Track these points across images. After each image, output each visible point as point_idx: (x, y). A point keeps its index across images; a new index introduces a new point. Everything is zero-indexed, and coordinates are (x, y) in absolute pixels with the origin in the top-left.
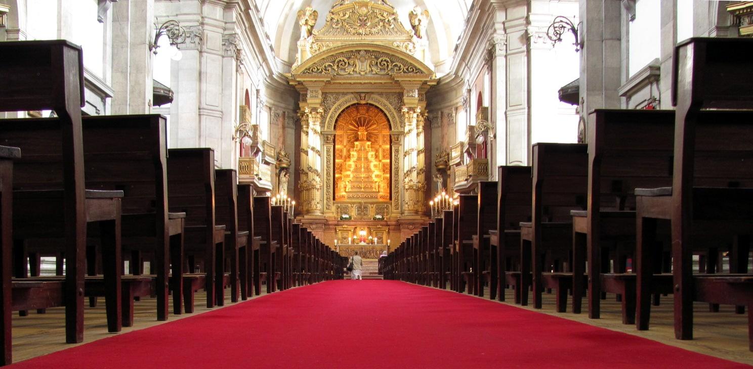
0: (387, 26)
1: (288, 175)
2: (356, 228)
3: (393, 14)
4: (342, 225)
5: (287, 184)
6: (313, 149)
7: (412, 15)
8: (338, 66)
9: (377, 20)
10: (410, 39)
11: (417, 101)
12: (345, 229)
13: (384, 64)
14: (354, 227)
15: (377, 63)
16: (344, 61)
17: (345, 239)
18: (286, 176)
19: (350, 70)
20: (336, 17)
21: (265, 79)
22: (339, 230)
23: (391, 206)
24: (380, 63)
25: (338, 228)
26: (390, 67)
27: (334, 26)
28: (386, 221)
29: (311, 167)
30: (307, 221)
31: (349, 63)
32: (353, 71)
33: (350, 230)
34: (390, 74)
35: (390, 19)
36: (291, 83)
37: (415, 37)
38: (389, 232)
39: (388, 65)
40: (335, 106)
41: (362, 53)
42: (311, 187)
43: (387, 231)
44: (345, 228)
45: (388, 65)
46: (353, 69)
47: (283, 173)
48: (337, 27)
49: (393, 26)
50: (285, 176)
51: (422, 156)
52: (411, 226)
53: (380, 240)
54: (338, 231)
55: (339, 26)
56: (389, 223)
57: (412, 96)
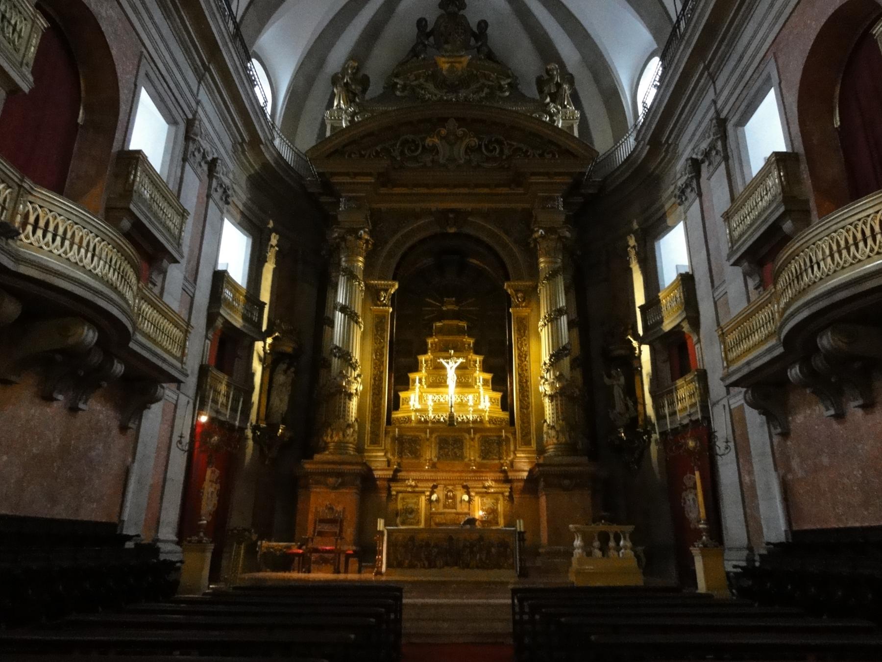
0: (498, 93)
1: (292, 369)
2: (435, 487)
3: (508, 77)
4: (405, 480)
5: (290, 388)
6: (344, 309)
7: (540, 83)
8: (402, 153)
9: (478, 85)
10: (545, 108)
11: (562, 218)
12: (409, 489)
13: (495, 148)
14: (431, 485)
15: (480, 146)
16: (414, 141)
17: (411, 513)
18: (289, 372)
19: (428, 159)
20: (400, 82)
21: (243, 151)
22: (398, 492)
23: (515, 438)
24: (486, 147)
25: (395, 488)
26: (506, 151)
27: (398, 93)
28: (505, 472)
29: (336, 347)
30: (320, 466)
31: (424, 146)
32: (433, 161)
33: (423, 492)
34: (506, 166)
35: (503, 83)
36: (310, 190)
37: (552, 105)
38: (511, 497)
39: (502, 151)
40: (398, 236)
41: (452, 124)
42: (332, 391)
43: (507, 494)
44: (411, 486)
45: (502, 151)
46: (431, 157)
47: (283, 366)
48: (402, 94)
49: (507, 94)
50: (285, 372)
51: (575, 331)
52: (567, 482)
53: (491, 516)
54: (394, 493)
55: (406, 93)
56: (511, 475)
57: (552, 208)
